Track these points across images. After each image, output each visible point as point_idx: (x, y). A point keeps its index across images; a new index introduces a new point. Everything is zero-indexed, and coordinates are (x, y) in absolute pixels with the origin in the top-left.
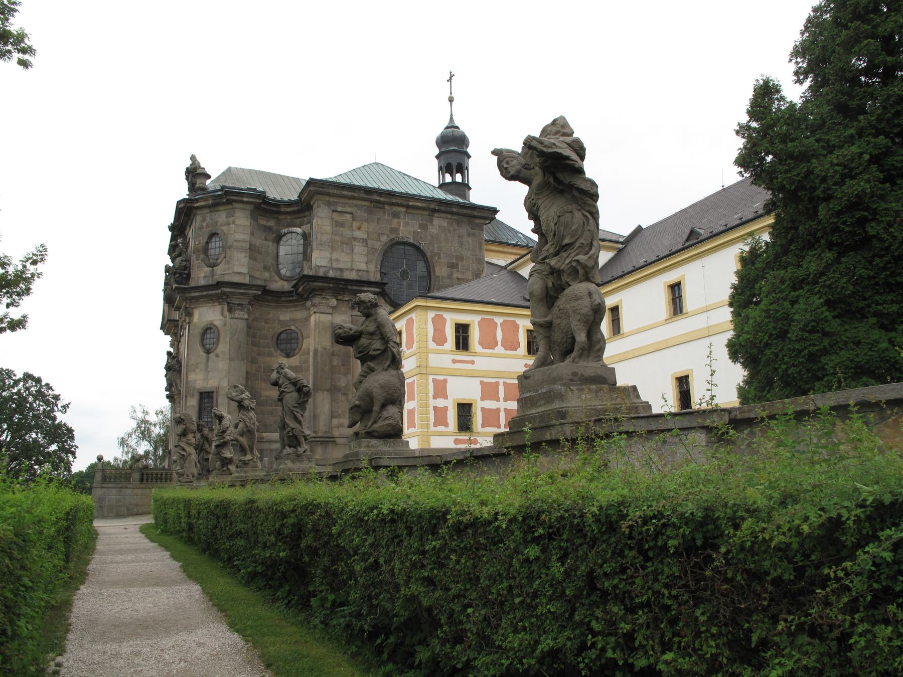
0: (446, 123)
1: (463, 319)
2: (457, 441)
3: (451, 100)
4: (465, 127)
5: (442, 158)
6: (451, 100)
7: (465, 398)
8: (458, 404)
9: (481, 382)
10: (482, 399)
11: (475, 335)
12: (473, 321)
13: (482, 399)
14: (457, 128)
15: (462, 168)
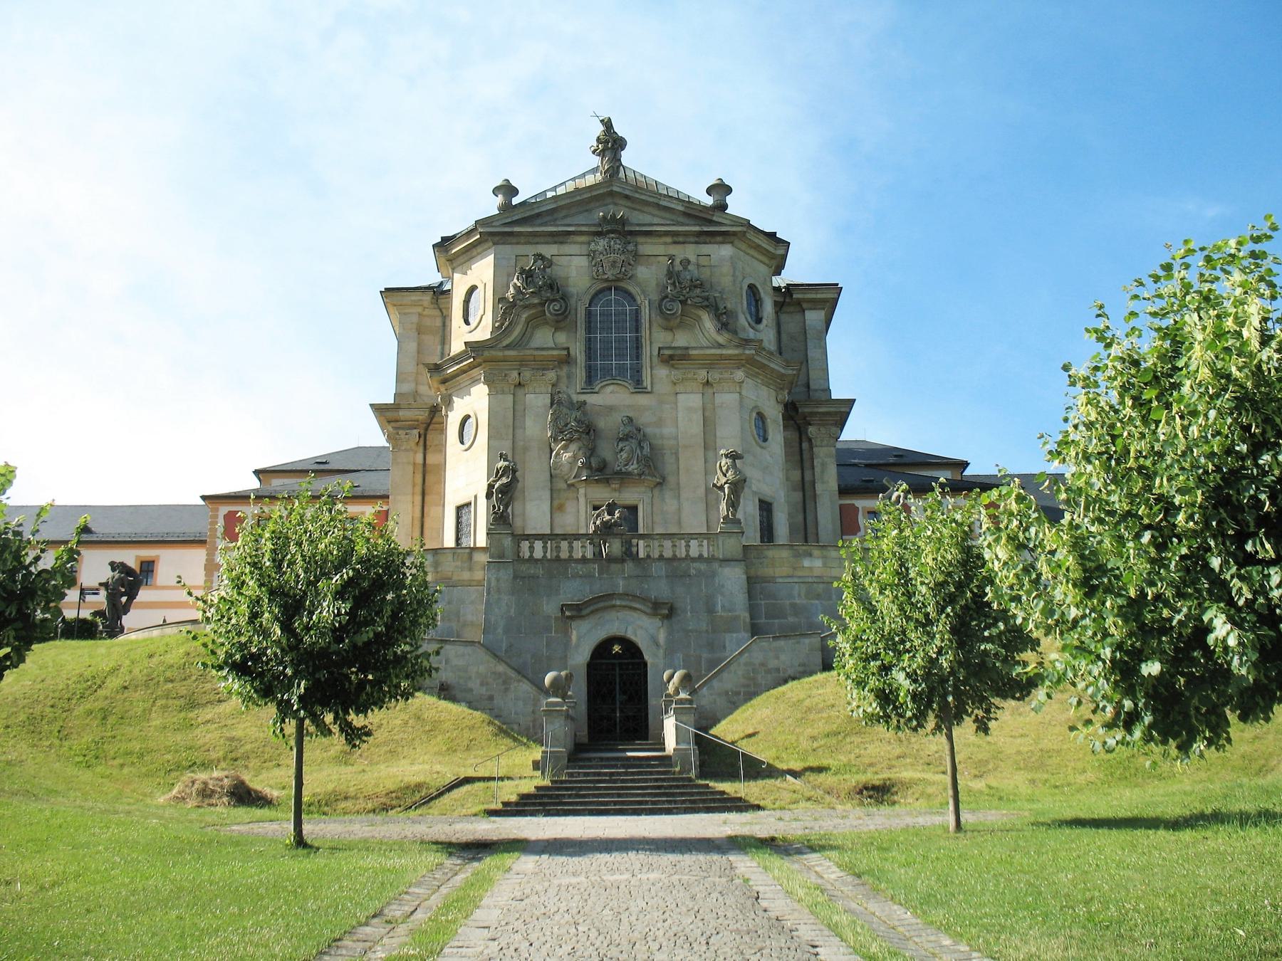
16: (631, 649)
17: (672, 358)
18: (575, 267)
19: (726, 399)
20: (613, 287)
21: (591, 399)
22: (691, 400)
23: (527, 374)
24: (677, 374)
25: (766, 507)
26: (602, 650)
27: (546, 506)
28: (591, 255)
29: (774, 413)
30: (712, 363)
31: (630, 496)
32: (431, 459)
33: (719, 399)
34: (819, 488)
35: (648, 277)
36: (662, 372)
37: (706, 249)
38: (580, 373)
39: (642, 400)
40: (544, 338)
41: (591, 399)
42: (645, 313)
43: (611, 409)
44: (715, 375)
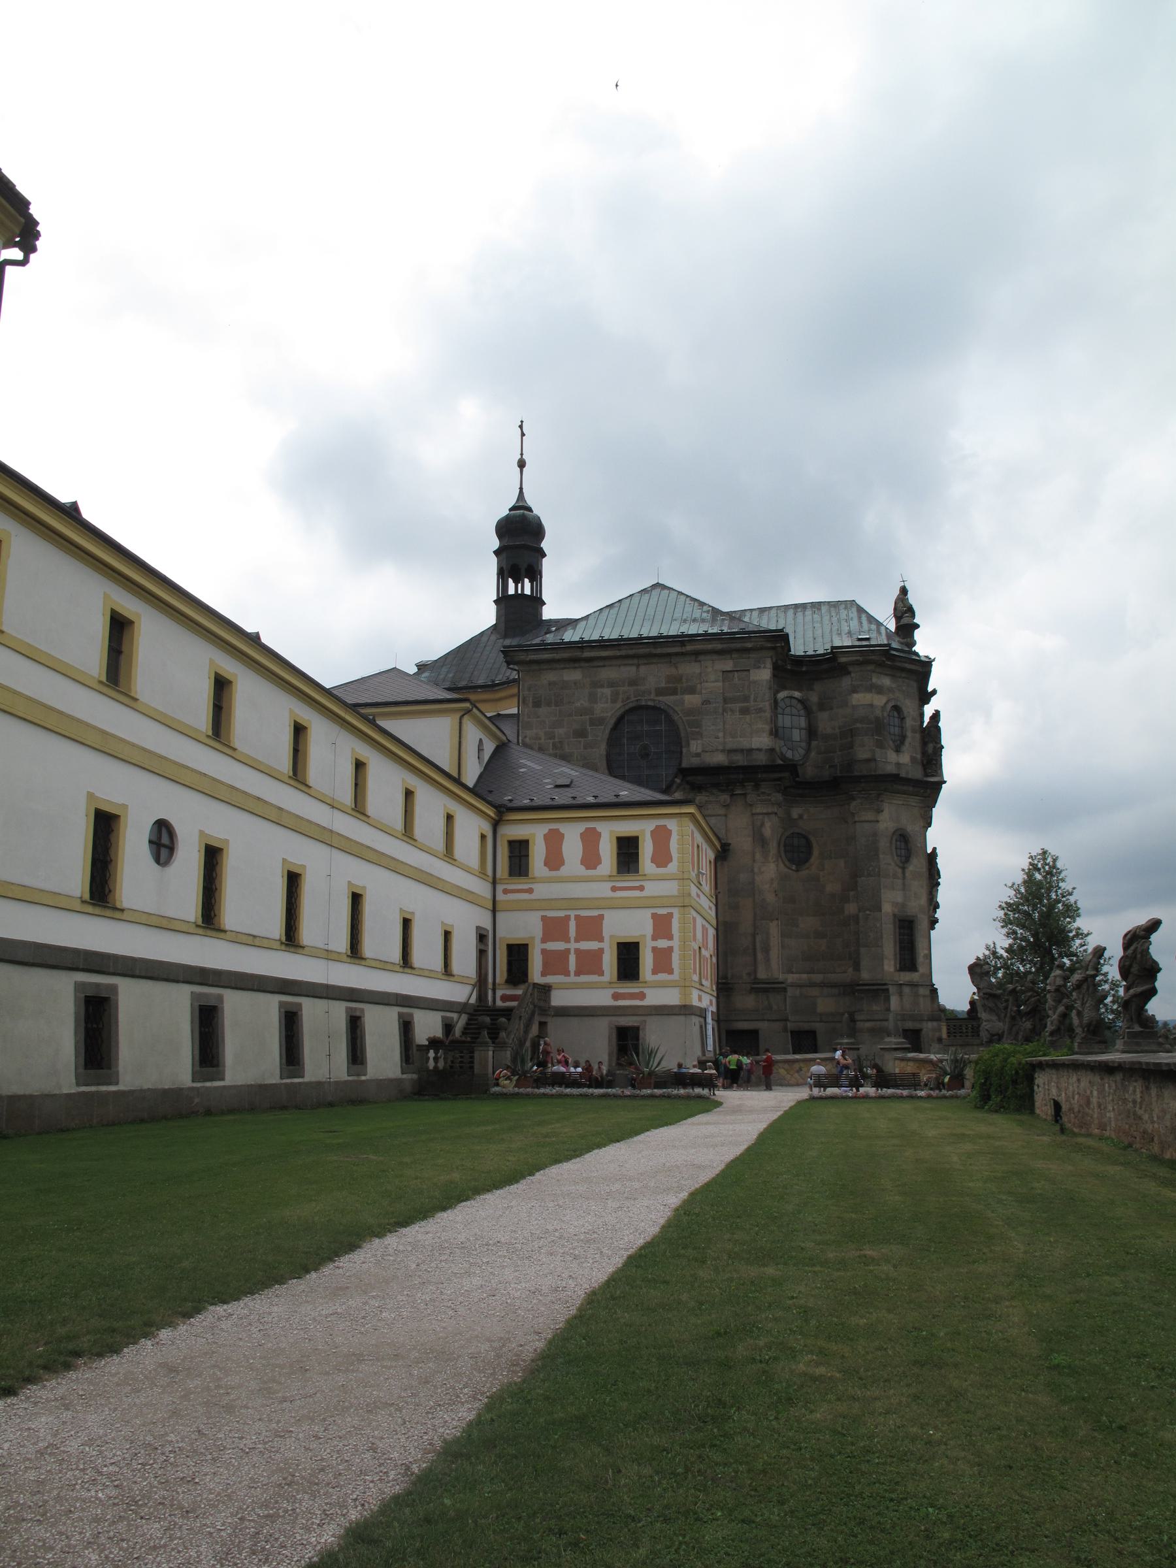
0: (512, 502)
1: (627, 828)
2: (616, 997)
3: (522, 464)
4: (539, 508)
5: (504, 555)
6: (522, 464)
7: (628, 935)
8: (619, 944)
9: (654, 916)
10: (654, 938)
11: (646, 849)
12: (643, 831)
13: (654, 938)
14: (530, 510)
15: (535, 575)
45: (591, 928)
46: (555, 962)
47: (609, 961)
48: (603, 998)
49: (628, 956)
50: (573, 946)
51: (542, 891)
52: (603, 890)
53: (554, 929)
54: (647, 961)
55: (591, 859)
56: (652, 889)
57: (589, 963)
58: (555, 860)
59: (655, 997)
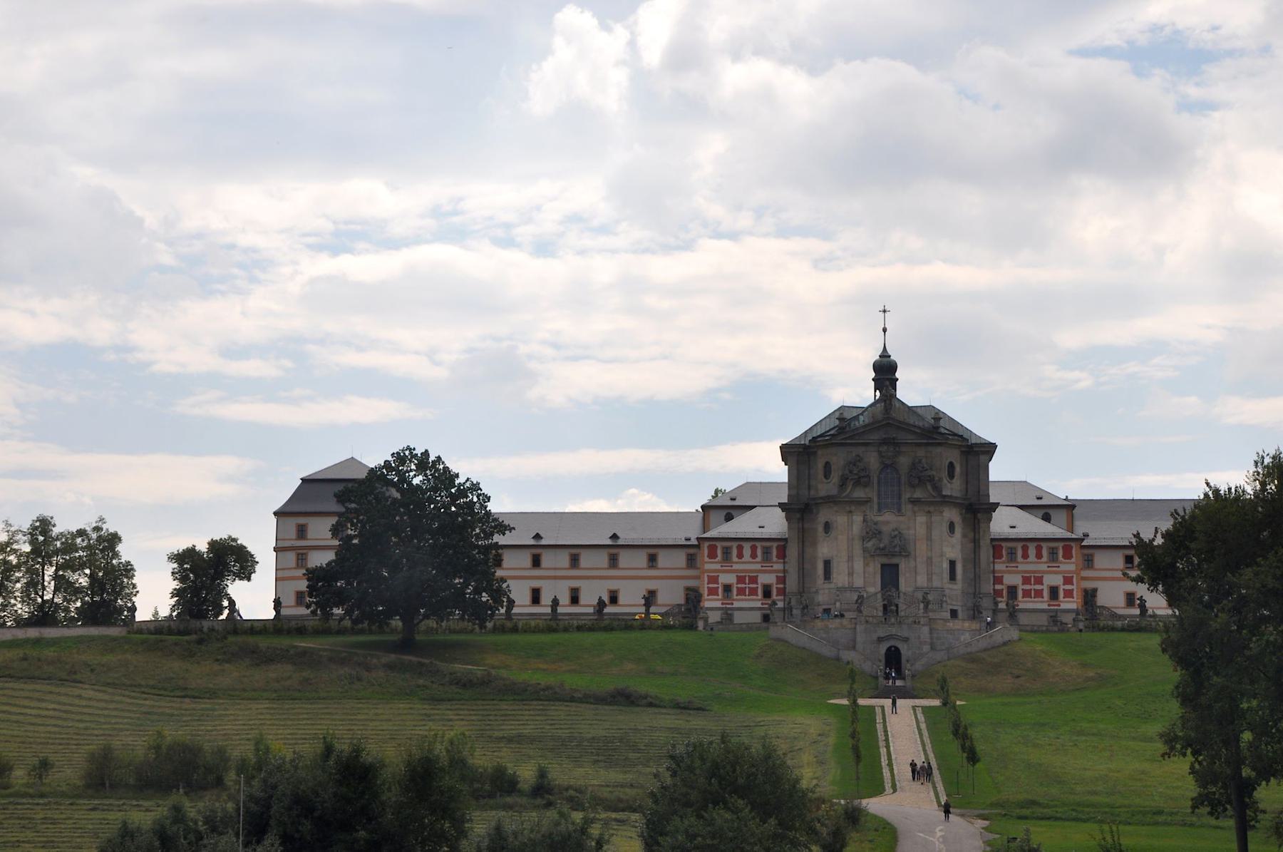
7: (1054, 583)
16: (897, 649)
17: (914, 502)
18: (872, 460)
19: (935, 518)
20: (888, 466)
21: (880, 519)
22: (921, 519)
23: (853, 508)
24: (916, 508)
25: (952, 564)
26: (889, 649)
27: (861, 563)
28: (880, 453)
29: (957, 519)
30: (931, 503)
31: (895, 561)
32: (806, 526)
33: (934, 518)
34: (982, 543)
35: (904, 461)
36: (910, 506)
37: (930, 448)
38: (876, 507)
39: (901, 518)
40: (859, 493)
41: (880, 519)
42: (903, 479)
43: (888, 522)
44: (932, 509)
45: (1039, 581)
46: (1027, 594)
47: (1046, 594)
48: (1045, 606)
49: (1054, 592)
50: (1033, 587)
51: (1022, 567)
52: (1044, 567)
53: (1026, 580)
54: (1061, 594)
55: (1039, 556)
56: (1063, 567)
57: (1039, 594)
58: (1025, 556)
59: (1064, 606)
